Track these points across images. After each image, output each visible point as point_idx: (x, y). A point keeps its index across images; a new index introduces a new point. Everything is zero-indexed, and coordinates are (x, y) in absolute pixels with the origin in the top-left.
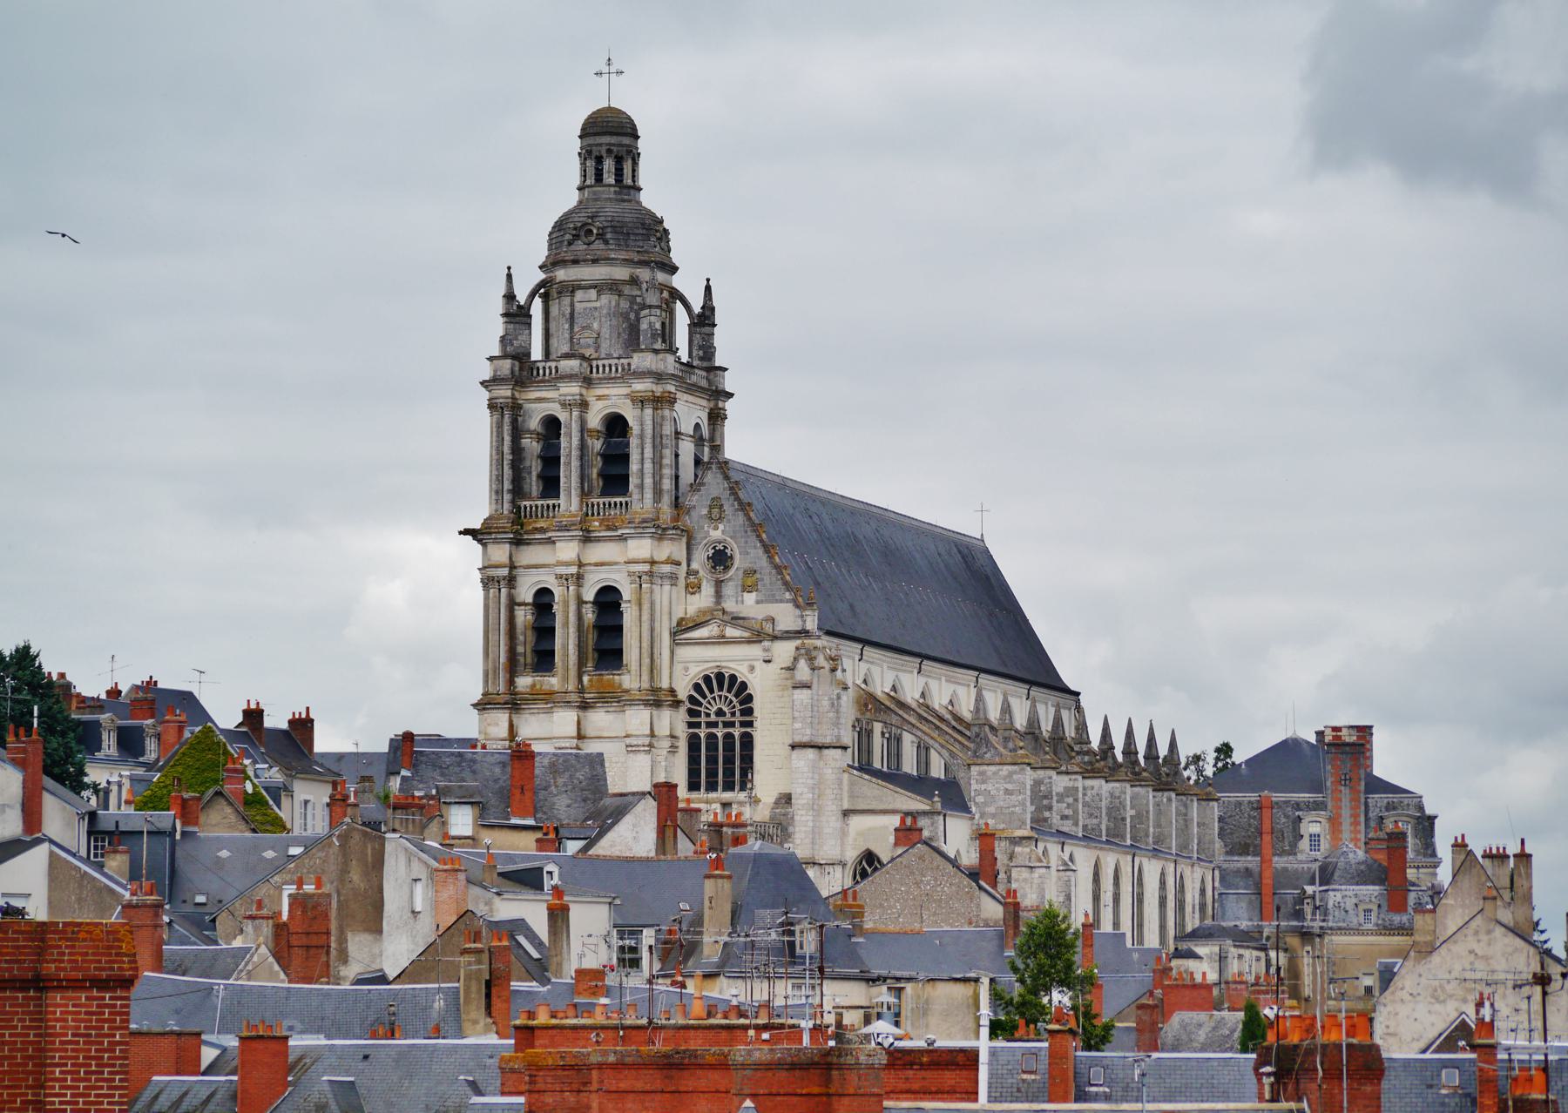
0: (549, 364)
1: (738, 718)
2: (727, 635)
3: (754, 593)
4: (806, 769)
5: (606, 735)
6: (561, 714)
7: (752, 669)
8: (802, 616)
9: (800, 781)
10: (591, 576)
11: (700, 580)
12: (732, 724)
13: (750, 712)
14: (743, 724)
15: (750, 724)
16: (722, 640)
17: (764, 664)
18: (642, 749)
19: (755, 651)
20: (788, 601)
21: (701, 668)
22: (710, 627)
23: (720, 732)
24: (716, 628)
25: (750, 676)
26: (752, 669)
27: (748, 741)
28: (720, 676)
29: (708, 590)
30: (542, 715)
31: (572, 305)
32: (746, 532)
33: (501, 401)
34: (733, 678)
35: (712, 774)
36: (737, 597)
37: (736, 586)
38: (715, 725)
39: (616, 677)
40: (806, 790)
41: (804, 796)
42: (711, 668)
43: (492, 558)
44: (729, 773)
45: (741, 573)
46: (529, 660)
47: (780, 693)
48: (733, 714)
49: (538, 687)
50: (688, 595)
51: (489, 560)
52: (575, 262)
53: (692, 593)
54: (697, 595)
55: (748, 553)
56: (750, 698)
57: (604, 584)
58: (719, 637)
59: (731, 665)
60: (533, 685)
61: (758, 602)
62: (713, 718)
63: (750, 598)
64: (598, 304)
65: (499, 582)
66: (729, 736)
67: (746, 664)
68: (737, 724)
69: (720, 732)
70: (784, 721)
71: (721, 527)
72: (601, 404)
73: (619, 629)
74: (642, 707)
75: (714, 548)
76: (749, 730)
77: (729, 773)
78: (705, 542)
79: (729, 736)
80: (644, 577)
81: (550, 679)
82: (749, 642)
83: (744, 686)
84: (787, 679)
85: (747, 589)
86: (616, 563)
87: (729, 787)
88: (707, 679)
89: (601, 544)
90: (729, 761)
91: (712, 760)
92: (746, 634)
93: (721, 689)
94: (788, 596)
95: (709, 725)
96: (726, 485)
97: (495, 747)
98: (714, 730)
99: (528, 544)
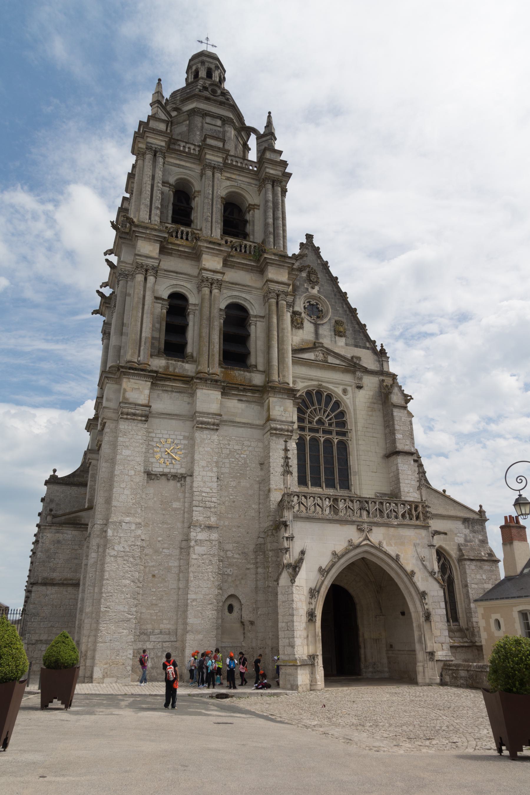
0: (188, 145)
1: (334, 428)
2: (329, 361)
3: (343, 339)
4: (409, 472)
5: (238, 420)
6: (204, 391)
7: (345, 391)
8: (379, 361)
9: (407, 481)
10: (225, 291)
11: (302, 319)
12: (330, 432)
13: (343, 424)
14: (338, 433)
15: (344, 434)
16: (325, 366)
17: (357, 390)
18: (286, 433)
19: (347, 378)
20: (368, 348)
21: (306, 384)
22: (317, 353)
23: (322, 438)
24: (321, 355)
25: (343, 396)
26: (345, 391)
27: (343, 447)
28: (319, 393)
29: (308, 326)
30: (174, 394)
31: (202, 123)
32: (335, 295)
33: (156, 146)
34: (329, 397)
35: (315, 470)
36: (331, 338)
37: (330, 330)
38: (317, 431)
39: (247, 374)
40: (411, 490)
41: (410, 494)
42: (314, 385)
43: (141, 251)
44: (330, 471)
45: (333, 321)
46: (162, 346)
47: (370, 413)
48: (330, 425)
49: (171, 369)
50: (293, 329)
51: (139, 251)
52: (207, 99)
53: (299, 328)
54: (301, 331)
55: (337, 310)
56: (342, 414)
57: (234, 300)
58: (323, 361)
59: (330, 386)
60: (167, 367)
61: (347, 345)
62: (315, 425)
63: (341, 341)
64: (221, 130)
65: (147, 271)
66: (328, 442)
67: (341, 387)
68: (334, 433)
69: (322, 438)
70: (374, 435)
71: (317, 288)
72: (228, 183)
73: (247, 336)
74: (285, 397)
75: (309, 302)
76: (344, 438)
77: (330, 471)
78: (305, 295)
79: (328, 442)
80: (282, 296)
81: (184, 364)
82: (346, 371)
83: (337, 404)
84: (374, 403)
85: (338, 333)
86: (248, 286)
87: (331, 484)
88: (309, 393)
89: (233, 270)
90: (329, 462)
91: (315, 459)
92: (344, 364)
93: (320, 403)
94: (368, 345)
95: (311, 430)
96: (319, 262)
97: (133, 411)
98: (317, 435)
99: (170, 254)
